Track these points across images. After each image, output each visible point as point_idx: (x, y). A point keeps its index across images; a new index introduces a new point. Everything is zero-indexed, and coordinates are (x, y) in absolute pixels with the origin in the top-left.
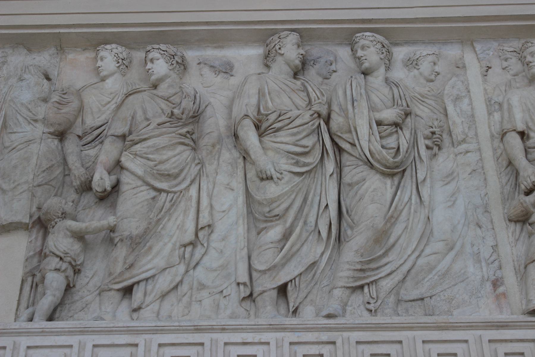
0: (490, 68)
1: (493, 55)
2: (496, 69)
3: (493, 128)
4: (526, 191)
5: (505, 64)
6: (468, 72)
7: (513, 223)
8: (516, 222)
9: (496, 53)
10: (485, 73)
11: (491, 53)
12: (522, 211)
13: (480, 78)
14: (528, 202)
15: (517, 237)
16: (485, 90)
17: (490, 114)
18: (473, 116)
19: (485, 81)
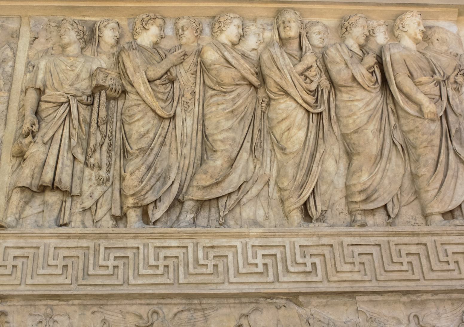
0: (37, 38)
1: (42, 28)
2: (42, 40)
3: (24, 84)
4: (26, 134)
5: (49, 36)
6: (20, 41)
7: (15, 158)
8: (17, 157)
9: (45, 27)
10: (32, 43)
11: (42, 27)
12: (18, 150)
13: (28, 45)
14: (23, 143)
15: (14, 169)
16: (28, 55)
17: (25, 74)
18: (12, 76)
19: (30, 48)
